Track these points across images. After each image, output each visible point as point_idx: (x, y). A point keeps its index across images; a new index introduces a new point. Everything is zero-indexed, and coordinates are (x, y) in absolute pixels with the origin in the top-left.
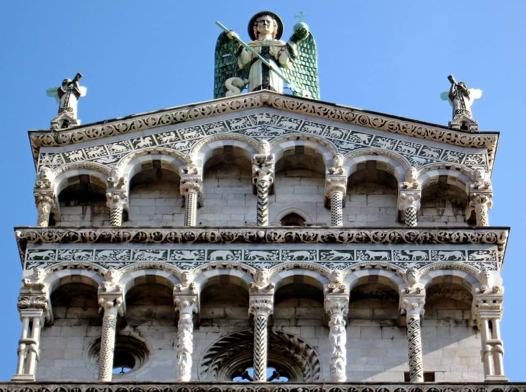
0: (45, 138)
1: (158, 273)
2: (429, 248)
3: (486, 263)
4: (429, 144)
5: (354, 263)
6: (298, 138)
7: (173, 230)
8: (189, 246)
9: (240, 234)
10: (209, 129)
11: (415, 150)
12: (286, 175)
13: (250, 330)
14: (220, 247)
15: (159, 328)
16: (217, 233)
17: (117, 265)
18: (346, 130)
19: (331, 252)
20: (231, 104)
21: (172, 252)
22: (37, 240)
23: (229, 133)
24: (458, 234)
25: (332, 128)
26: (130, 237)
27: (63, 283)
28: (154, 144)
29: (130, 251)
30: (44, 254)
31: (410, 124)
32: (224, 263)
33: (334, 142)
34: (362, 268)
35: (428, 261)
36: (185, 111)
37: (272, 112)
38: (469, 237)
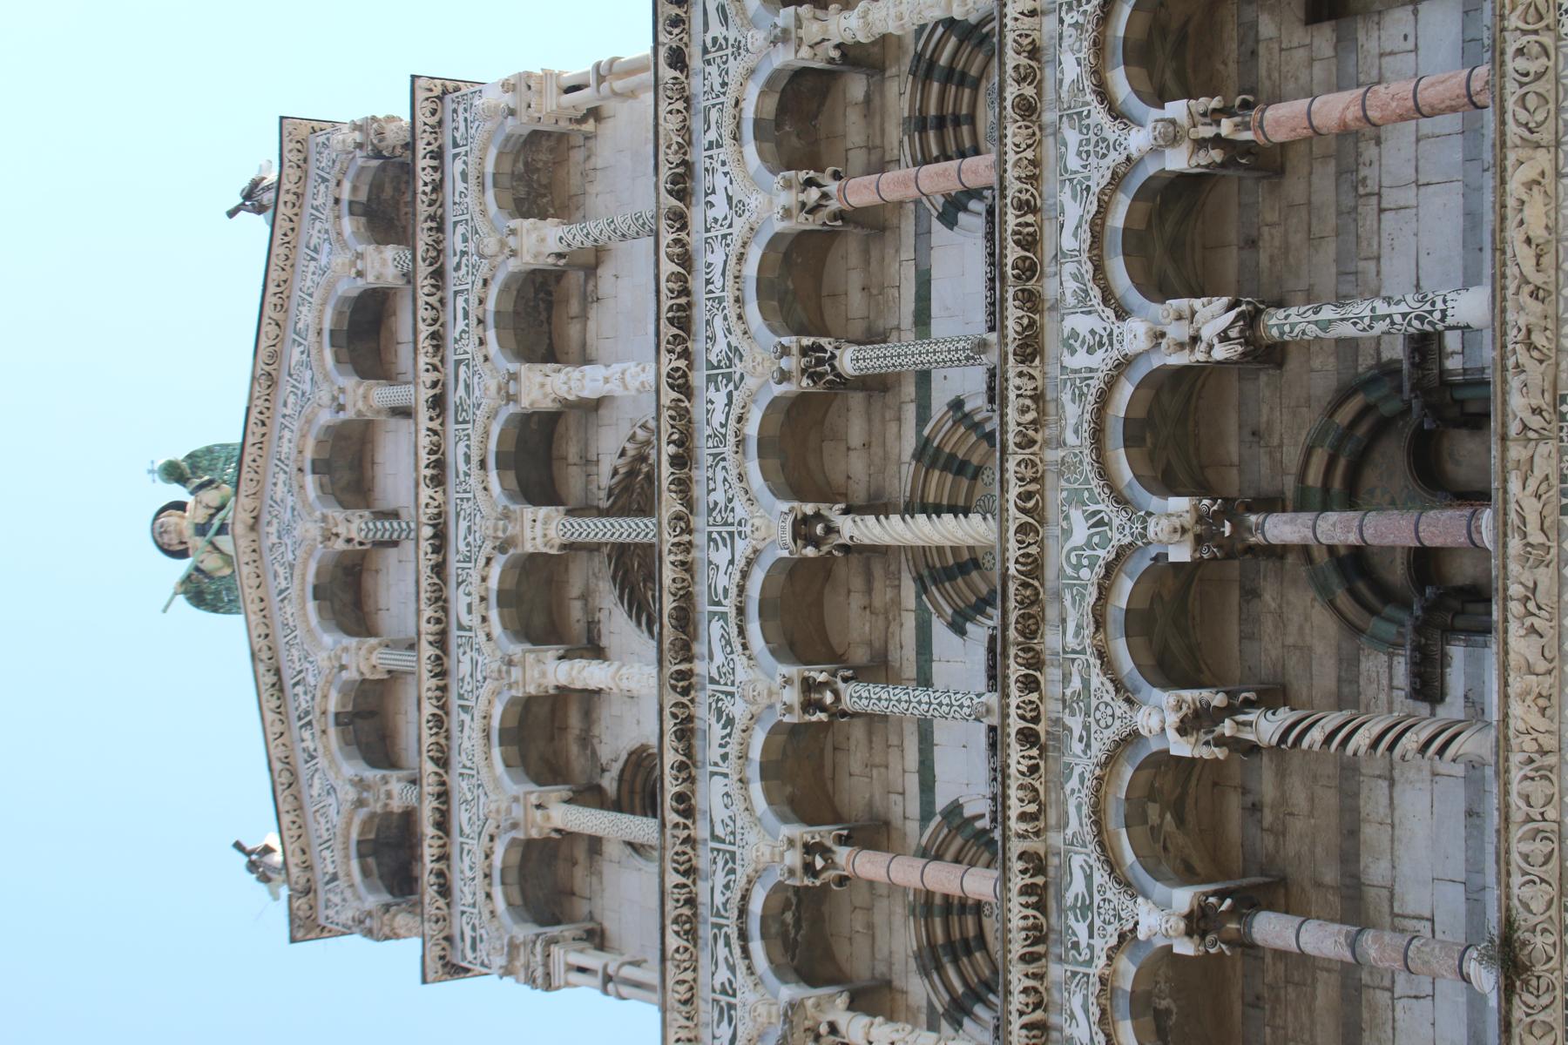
0: (301, 913)
1: (496, 723)
2: (450, 220)
4: (303, 239)
7: (425, 694)
8: (450, 663)
12: (371, 490)
13: (606, 550)
14: (452, 607)
15: (603, 723)
16: (428, 612)
18: (285, 388)
21: (461, 697)
22: (444, 944)
23: (294, 592)
26: (436, 774)
27: (518, 900)
29: (461, 774)
30: (468, 933)
31: (273, 275)
32: (476, 600)
34: (482, 342)
36: (262, 668)
37: (265, 518)
38: (429, 148)
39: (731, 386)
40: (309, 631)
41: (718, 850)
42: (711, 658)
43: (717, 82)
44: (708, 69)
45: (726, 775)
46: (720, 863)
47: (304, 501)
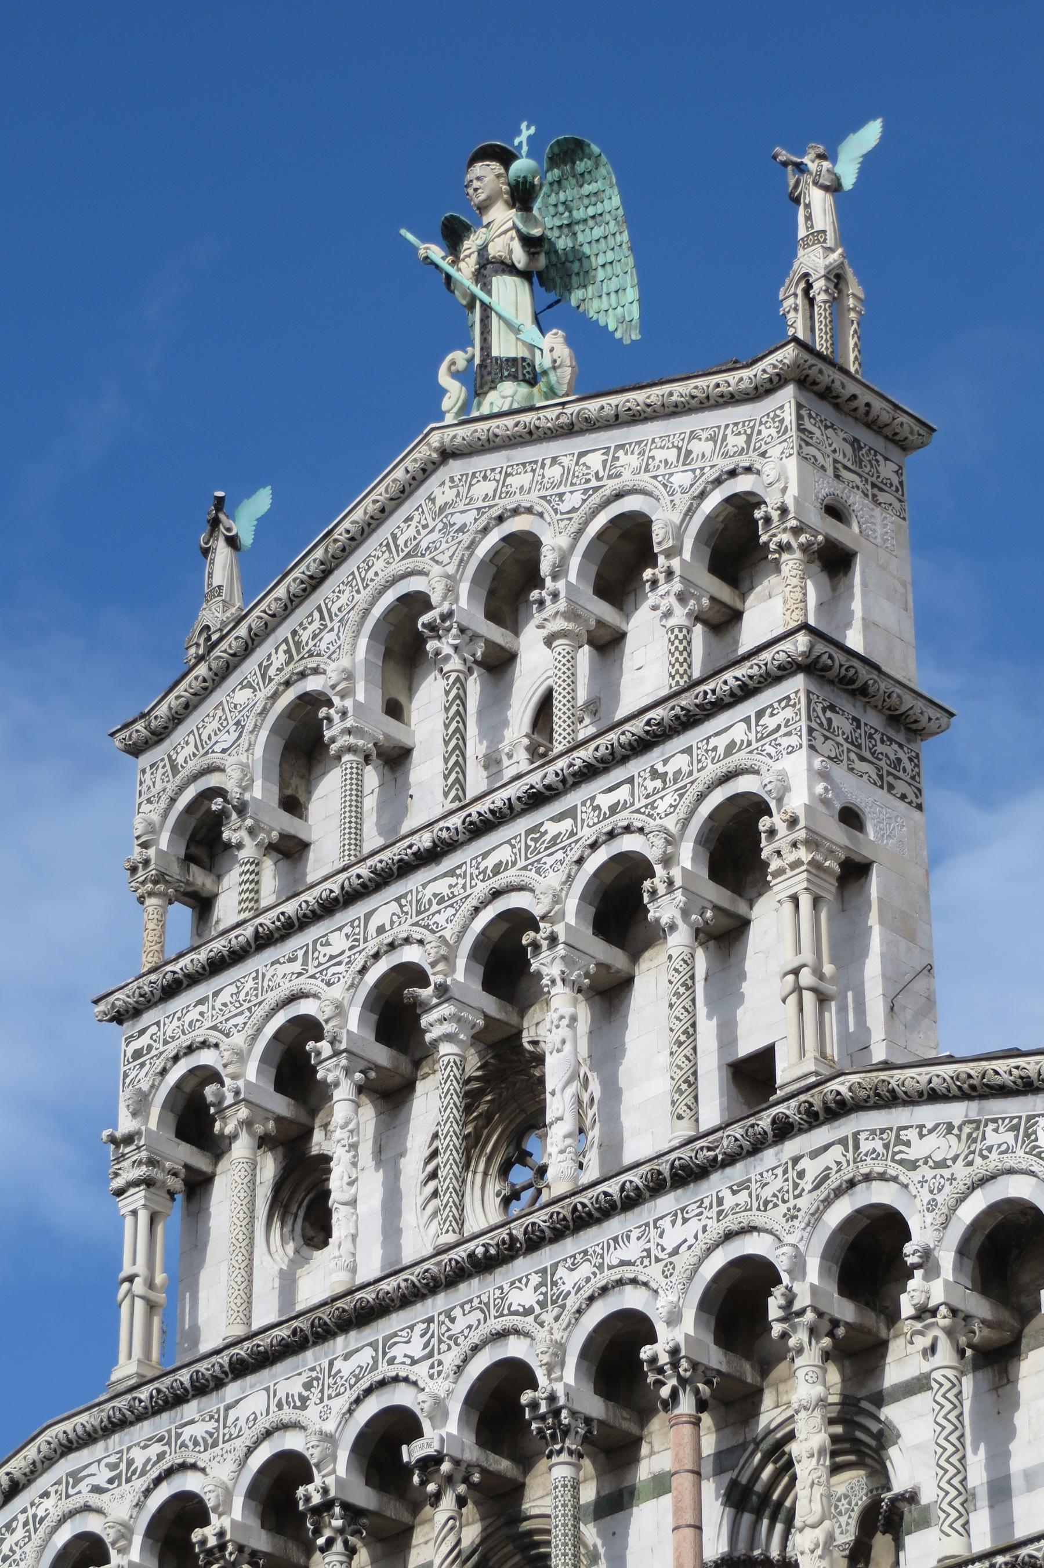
0: (134, 735)
3: (785, 735)
5: (576, 842)
6: (500, 519)
9: (396, 858)
10: (367, 571)
11: (675, 451)
17: (240, 1020)
19: (542, 830)
20: (386, 491)
22: (131, 1012)
24: (725, 683)
25: (548, 462)
28: (291, 658)
29: (257, 971)
30: (144, 1041)
33: (549, 502)
34: (594, 846)
35: (691, 779)
39: (537, 1309)
40: (367, 612)
41: (218, 1421)
42: (347, 1357)
43: (767, 1193)
44: (779, 1171)
45: (268, 1414)
46: (211, 1426)
47: (472, 545)
